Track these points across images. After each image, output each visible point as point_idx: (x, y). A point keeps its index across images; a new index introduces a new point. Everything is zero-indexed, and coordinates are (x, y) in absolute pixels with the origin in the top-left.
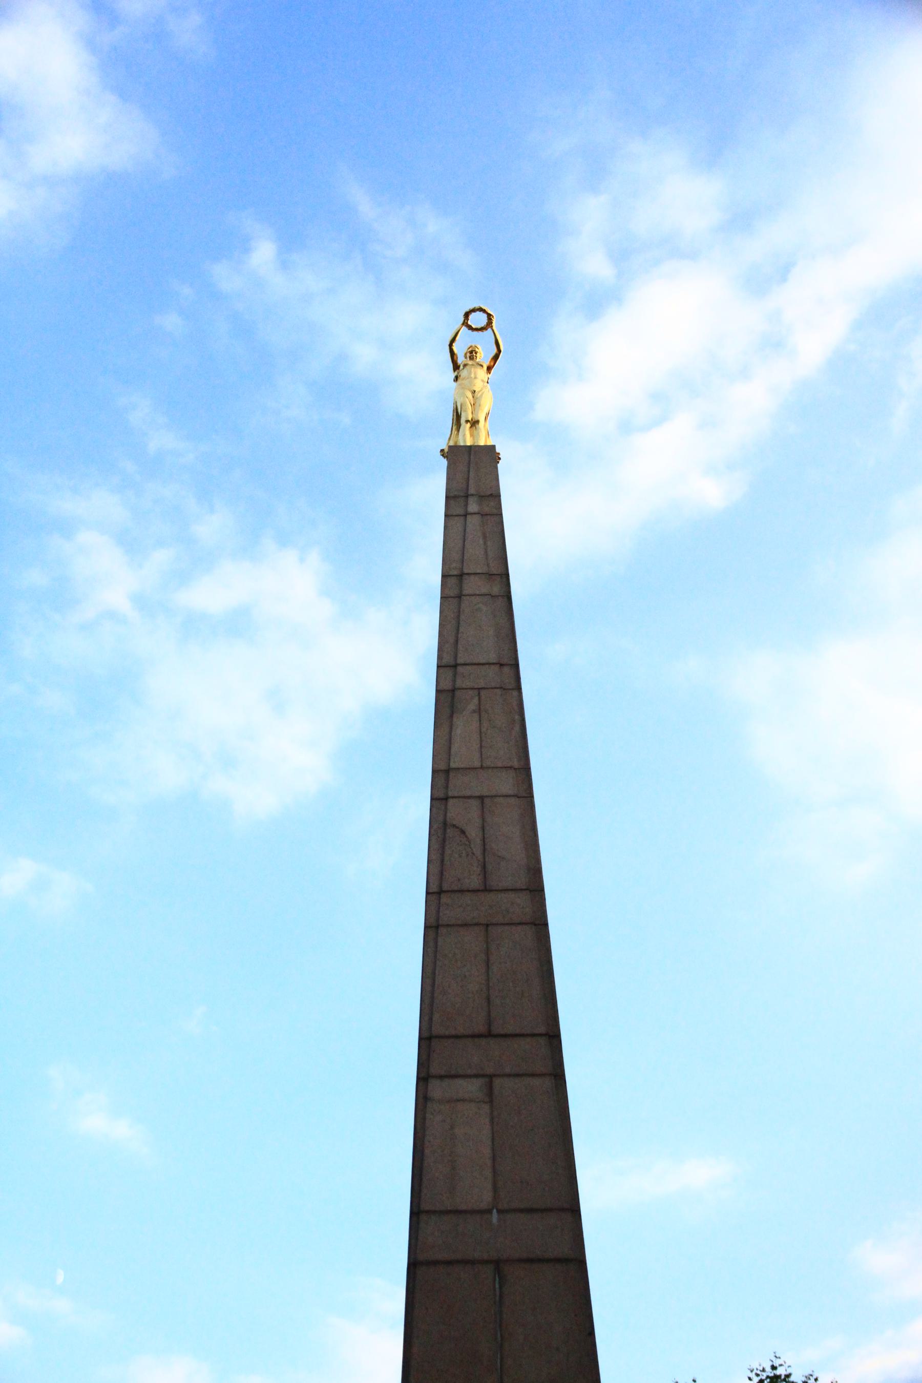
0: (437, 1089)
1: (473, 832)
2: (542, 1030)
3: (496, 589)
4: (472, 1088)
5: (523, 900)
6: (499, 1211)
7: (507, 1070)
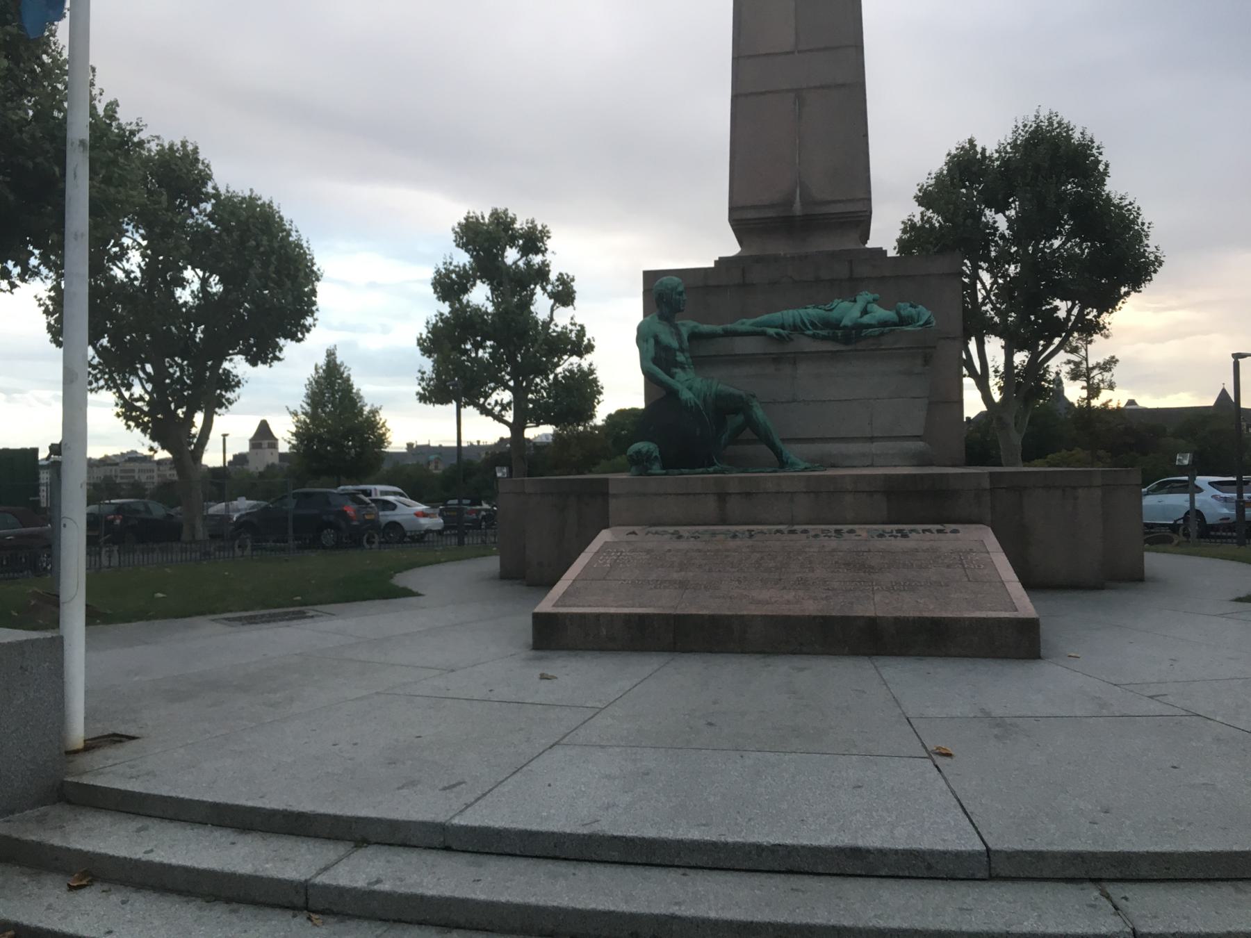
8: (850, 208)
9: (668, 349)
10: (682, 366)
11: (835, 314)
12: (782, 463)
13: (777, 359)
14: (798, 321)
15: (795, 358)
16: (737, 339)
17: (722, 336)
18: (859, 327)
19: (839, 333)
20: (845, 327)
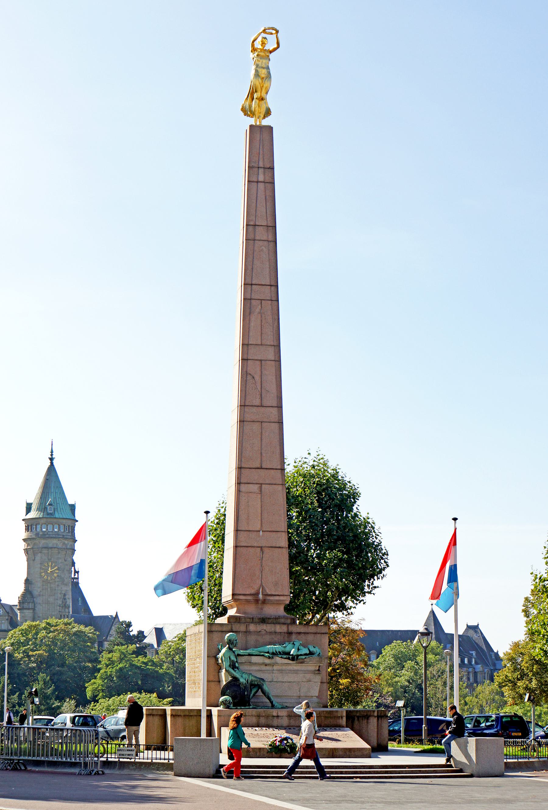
0: (243, 488)
1: (257, 378)
2: (279, 467)
3: (271, 238)
4: (255, 488)
5: (275, 411)
6: (263, 531)
7: (267, 482)
9: (233, 661)
11: (287, 650)
12: (273, 706)
14: (274, 652)
15: (273, 665)
16: (252, 657)
19: (291, 657)
20: (292, 655)
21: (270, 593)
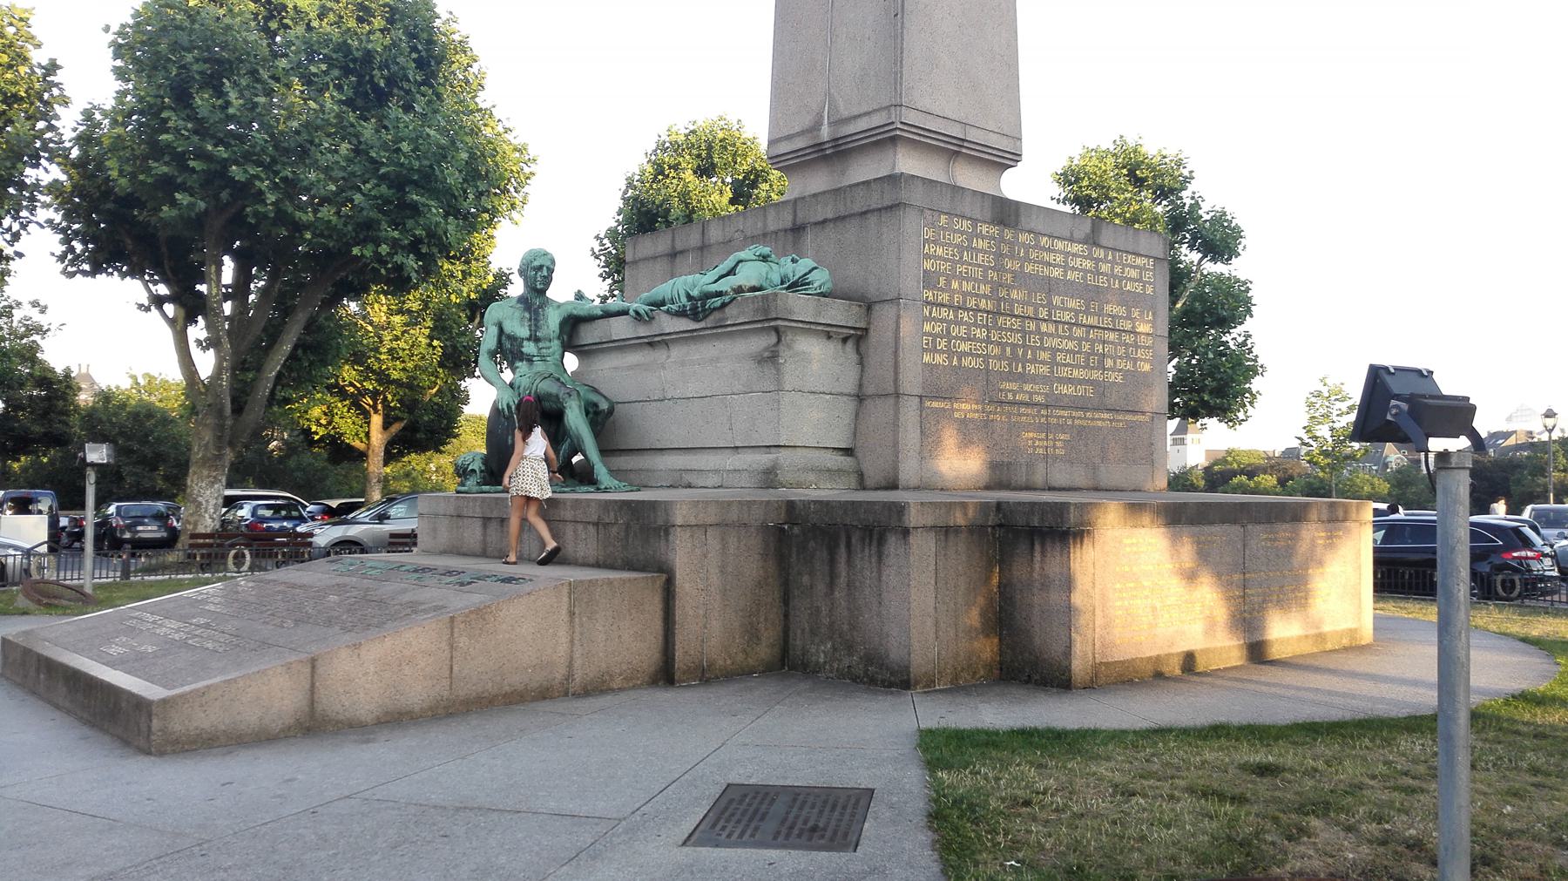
8: (877, 120)
10: (530, 360)
13: (652, 344)
17: (601, 317)
18: (707, 296)
21: (846, 114)
